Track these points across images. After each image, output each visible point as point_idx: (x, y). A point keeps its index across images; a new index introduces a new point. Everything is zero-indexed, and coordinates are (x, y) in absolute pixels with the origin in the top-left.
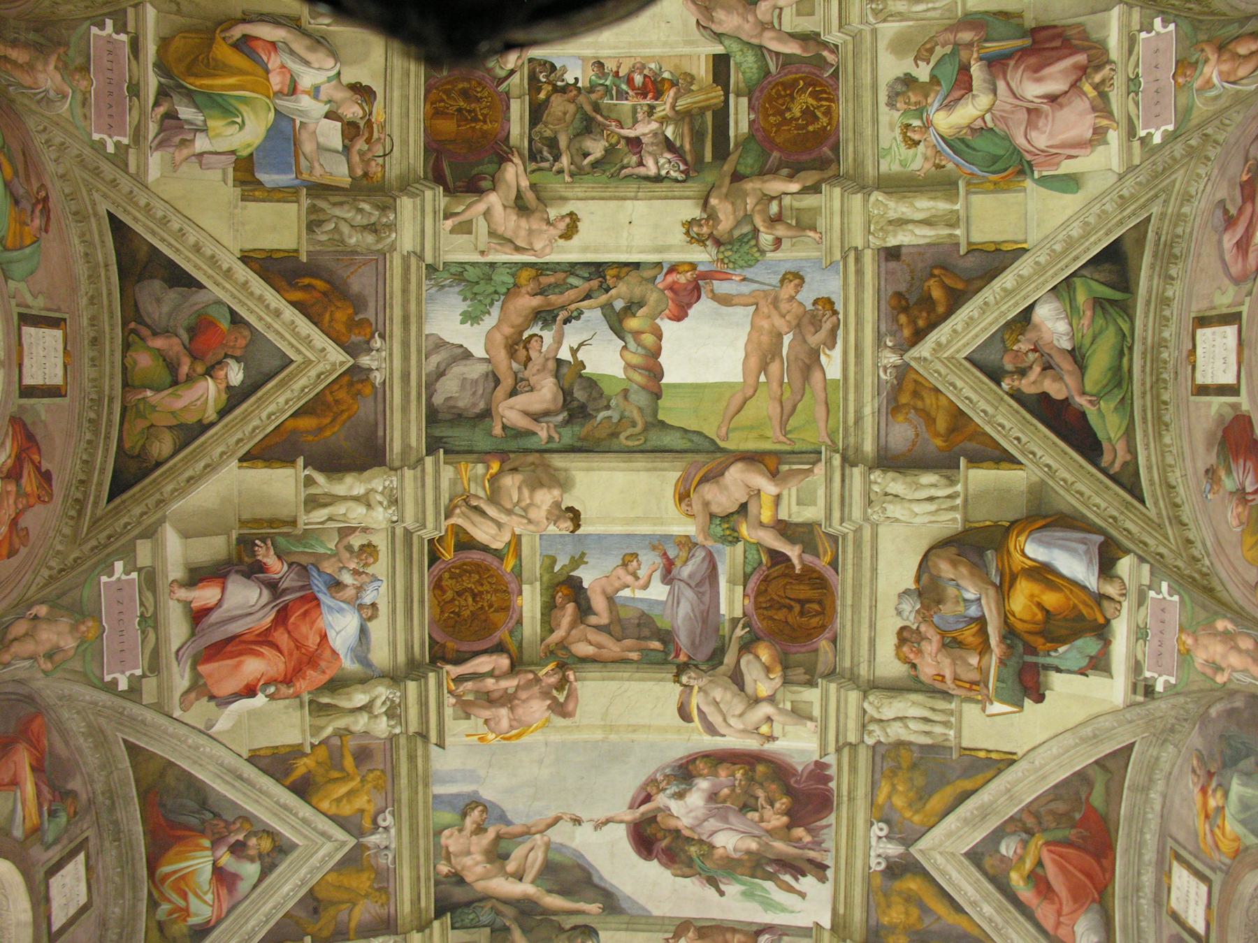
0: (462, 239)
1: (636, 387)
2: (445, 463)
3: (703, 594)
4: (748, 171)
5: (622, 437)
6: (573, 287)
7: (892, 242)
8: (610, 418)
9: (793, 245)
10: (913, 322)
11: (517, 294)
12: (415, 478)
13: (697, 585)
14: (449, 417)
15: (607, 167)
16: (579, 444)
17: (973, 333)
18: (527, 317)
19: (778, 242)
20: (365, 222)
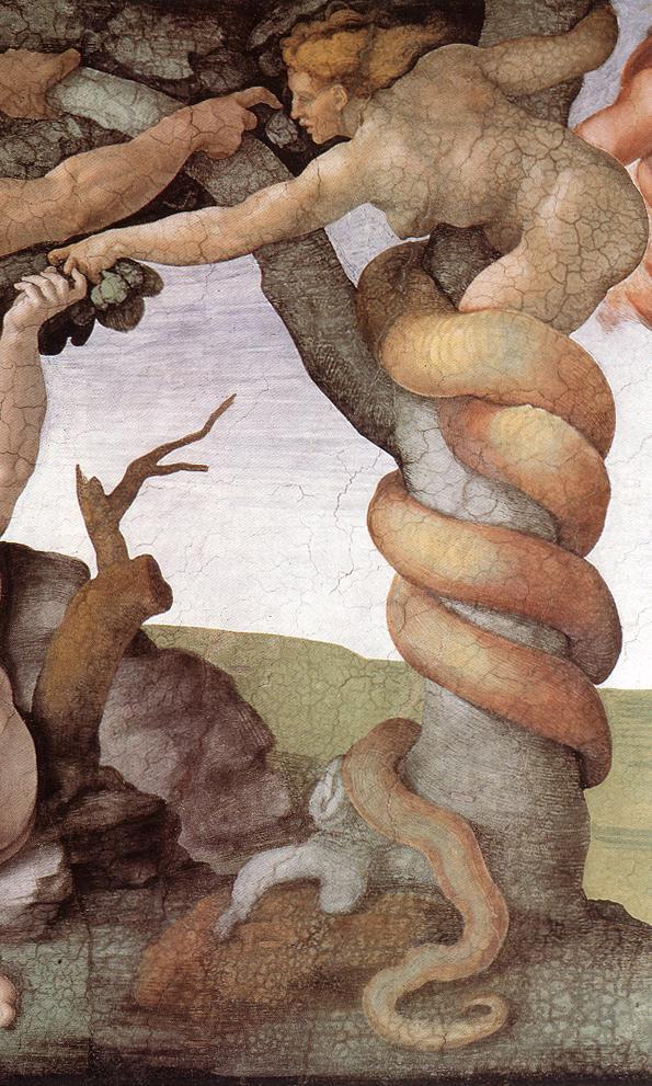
1: (454, 708)
5: (378, 996)
6: (95, 136)
8: (311, 884)
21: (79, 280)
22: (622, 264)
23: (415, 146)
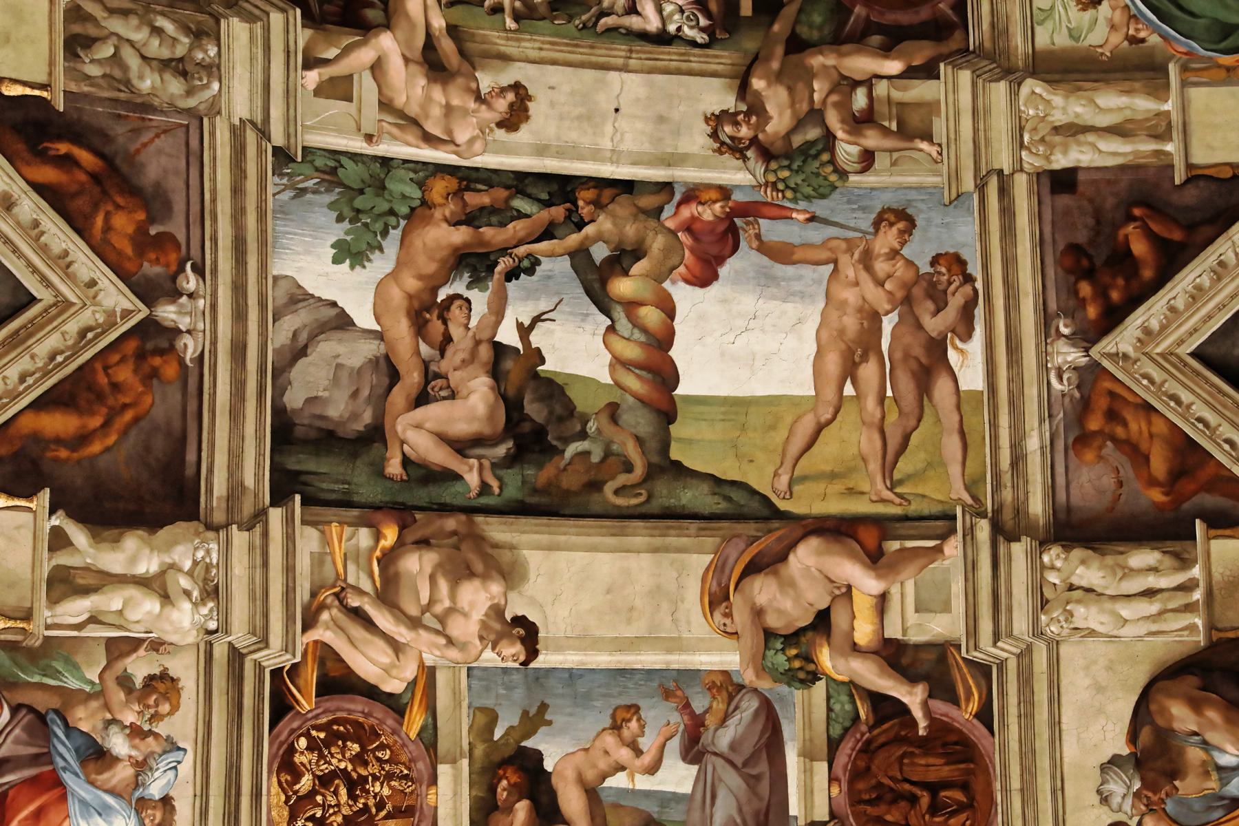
0: (336, 108)
1: (631, 399)
2: (304, 522)
3: (757, 778)
4: (815, 35)
5: (609, 488)
6: (521, 215)
7: (1060, 162)
8: (586, 454)
9: (894, 164)
10: (1102, 293)
11: (428, 221)
12: (251, 548)
13: (745, 764)
14: (313, 434)
15: (577, 9)
16: (534, 500)
17: (1203, 312)
18: (443, 262)
19: (868, 159)
20: (165, 54)
21: (516, 260)
22: (677, 263)
23: (615, 225)
